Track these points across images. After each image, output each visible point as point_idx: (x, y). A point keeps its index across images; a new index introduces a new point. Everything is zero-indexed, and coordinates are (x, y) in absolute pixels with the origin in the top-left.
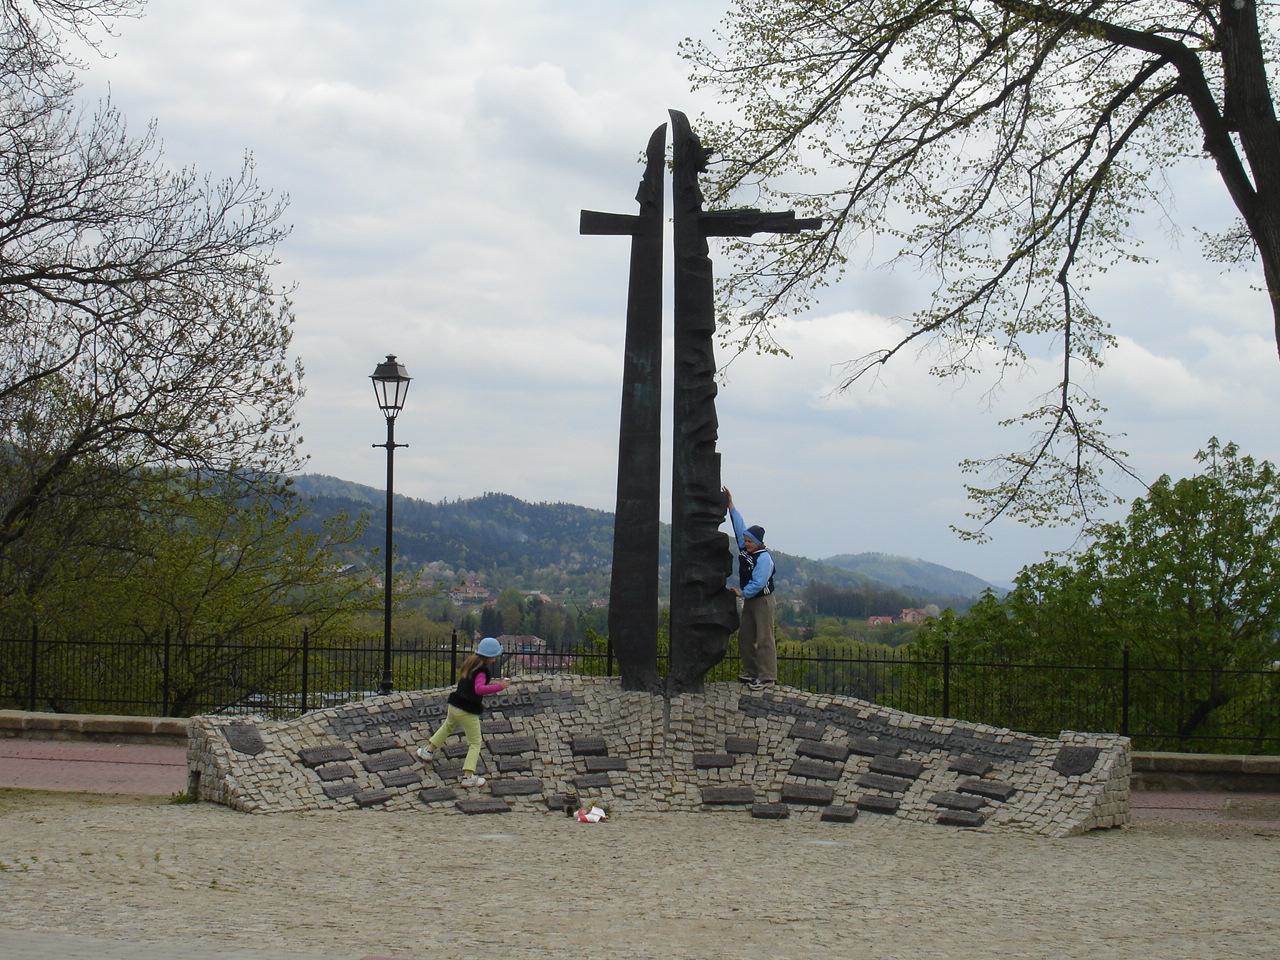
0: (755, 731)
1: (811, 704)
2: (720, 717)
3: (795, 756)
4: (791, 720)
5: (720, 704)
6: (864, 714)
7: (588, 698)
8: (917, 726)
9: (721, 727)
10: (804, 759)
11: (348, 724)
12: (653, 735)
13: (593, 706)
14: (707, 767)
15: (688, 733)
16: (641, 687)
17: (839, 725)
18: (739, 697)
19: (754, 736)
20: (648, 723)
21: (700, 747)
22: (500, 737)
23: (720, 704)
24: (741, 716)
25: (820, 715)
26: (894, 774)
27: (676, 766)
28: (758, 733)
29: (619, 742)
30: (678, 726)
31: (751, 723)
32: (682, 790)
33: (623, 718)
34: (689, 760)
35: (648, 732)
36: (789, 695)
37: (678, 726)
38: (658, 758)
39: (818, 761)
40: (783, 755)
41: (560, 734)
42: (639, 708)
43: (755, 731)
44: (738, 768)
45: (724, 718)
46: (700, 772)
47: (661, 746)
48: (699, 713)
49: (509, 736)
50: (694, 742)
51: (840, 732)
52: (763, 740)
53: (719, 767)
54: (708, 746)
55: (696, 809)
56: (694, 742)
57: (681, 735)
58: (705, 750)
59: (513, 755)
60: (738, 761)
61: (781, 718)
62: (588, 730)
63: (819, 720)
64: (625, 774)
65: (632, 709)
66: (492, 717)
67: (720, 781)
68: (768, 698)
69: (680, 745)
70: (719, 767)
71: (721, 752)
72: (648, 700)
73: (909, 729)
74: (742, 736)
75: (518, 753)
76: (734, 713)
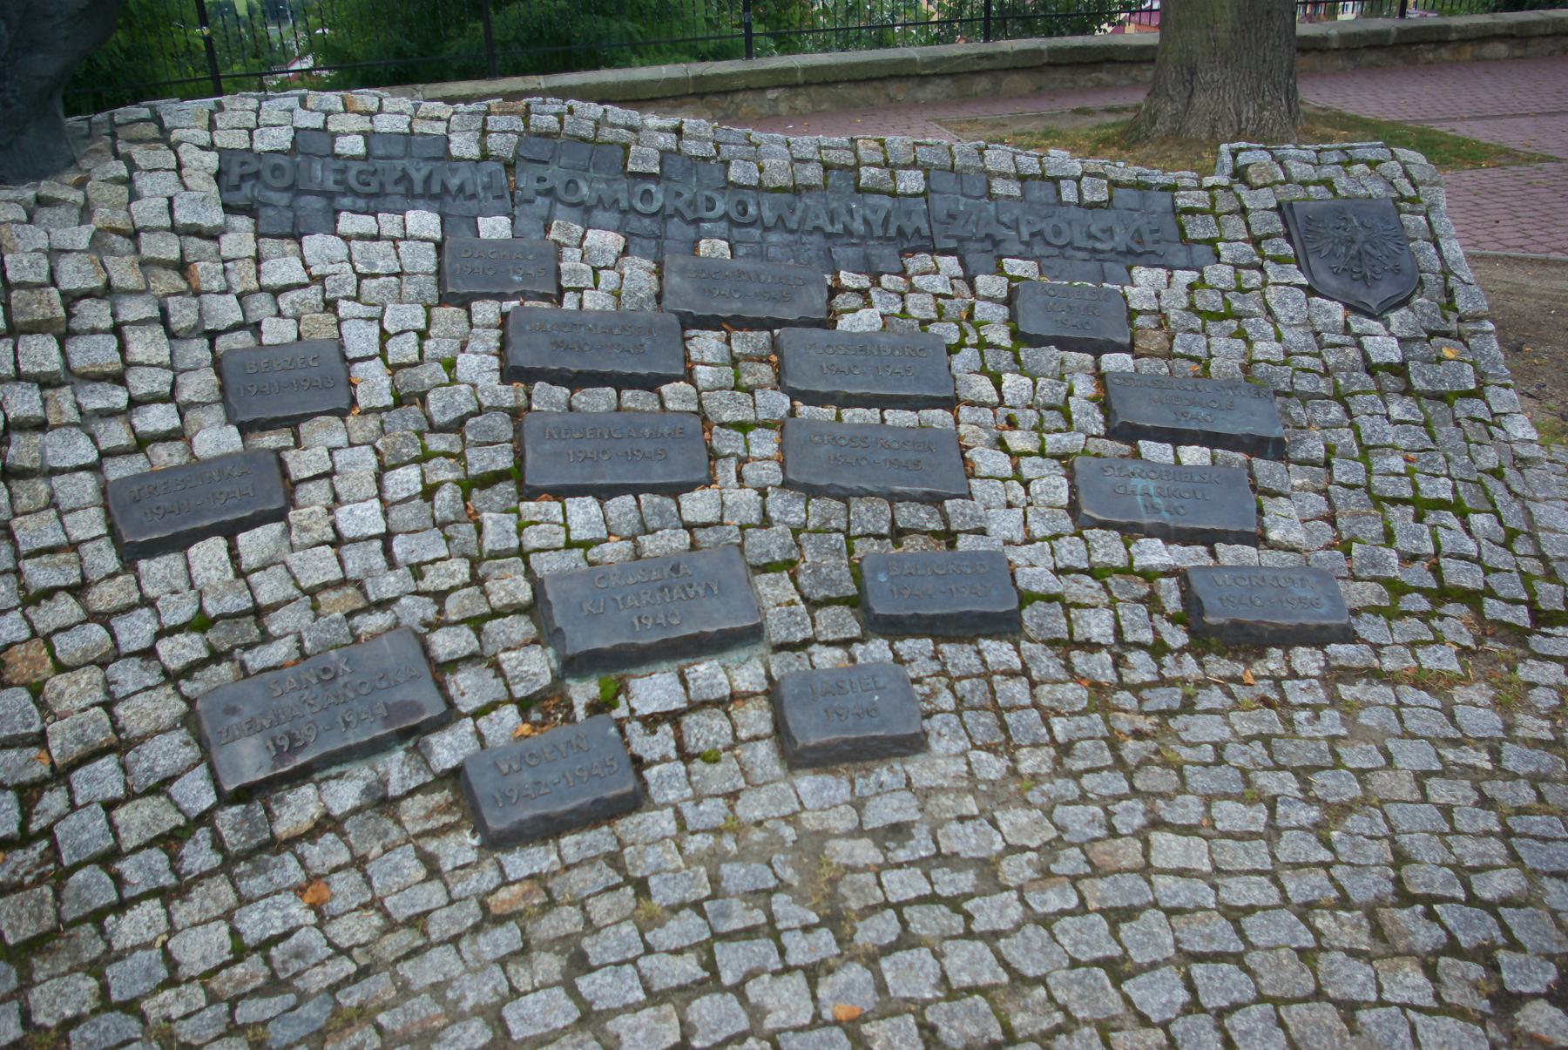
0: (313, 295)
2: (166, 265)
3: (509, 395)
4: (424, 221)
5: (149, 210)
6: (644, 159)
8: (812, 174)
10: (549, 397)
14: (180, 543)
15: (46, 383)
17: (586, 213)
18: (212, 160)
19: (320, 327)
21: (116, 434)
23: (149, 210)
24: (240, 239)
25: (505, 179)
26: (883, 402)
27: (40, 575)
28: (330, 306)
31: (283, 268)
32: (98, 729)
34: (88, 524)
36: (384, 124)
39: (599, 400)
40: (462, 400)
43: (313, 295)
45: (182, 267)
46: (156, 570)
48: (75, 275)
50: (87, 420)
52: (360, 339)
53: (229, 531)
54: (158, 418)
55: (199, 855)
56: (87, 420)
58: (142, 443)
60: (301, 464)
61: (389, 223)
63: (511, 203)
67: (258, 612)
68: (311, 144)
70: (229, 531)
71: (216, 438)
73: (796, 190)
74: (278, 331)
76: (213, 235)
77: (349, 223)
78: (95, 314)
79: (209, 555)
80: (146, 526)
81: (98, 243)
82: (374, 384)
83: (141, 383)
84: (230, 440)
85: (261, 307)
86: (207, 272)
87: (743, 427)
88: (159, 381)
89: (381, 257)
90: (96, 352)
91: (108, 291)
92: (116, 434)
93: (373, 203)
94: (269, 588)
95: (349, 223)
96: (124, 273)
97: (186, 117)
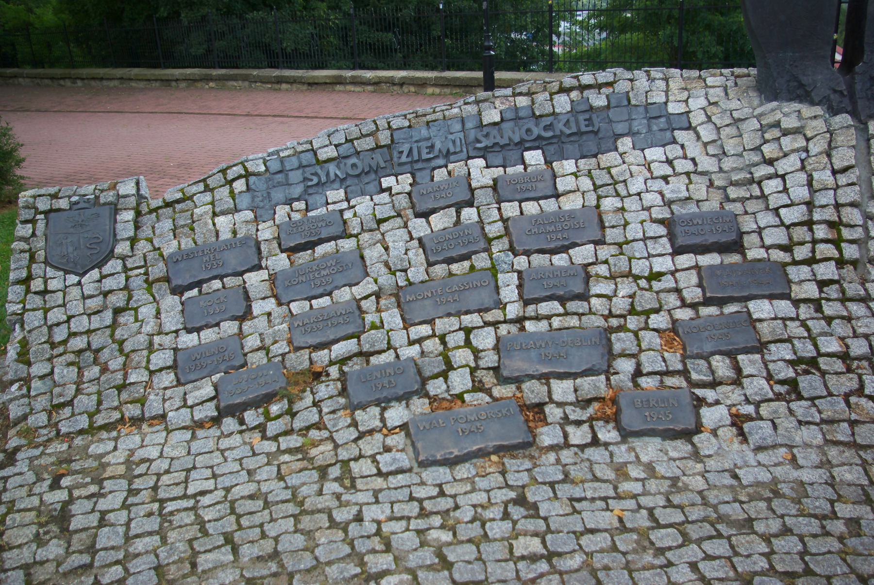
7: (697, 118)
11: (280, 184)
13: (706, 133)
16: (803, 95)
20: (824, 177)
22: (531, 208)
29: (766, 219)
33: (770, 162)
38: (854, 263)
41: (651, 198)
42: (801, 143)
47: (858, 233)
49: (550, 205)
59: (553, 252)
62: (700, 189)
65: (787, 143)
66: (523, 162)
72: (819, 125)
75: (564, 249)
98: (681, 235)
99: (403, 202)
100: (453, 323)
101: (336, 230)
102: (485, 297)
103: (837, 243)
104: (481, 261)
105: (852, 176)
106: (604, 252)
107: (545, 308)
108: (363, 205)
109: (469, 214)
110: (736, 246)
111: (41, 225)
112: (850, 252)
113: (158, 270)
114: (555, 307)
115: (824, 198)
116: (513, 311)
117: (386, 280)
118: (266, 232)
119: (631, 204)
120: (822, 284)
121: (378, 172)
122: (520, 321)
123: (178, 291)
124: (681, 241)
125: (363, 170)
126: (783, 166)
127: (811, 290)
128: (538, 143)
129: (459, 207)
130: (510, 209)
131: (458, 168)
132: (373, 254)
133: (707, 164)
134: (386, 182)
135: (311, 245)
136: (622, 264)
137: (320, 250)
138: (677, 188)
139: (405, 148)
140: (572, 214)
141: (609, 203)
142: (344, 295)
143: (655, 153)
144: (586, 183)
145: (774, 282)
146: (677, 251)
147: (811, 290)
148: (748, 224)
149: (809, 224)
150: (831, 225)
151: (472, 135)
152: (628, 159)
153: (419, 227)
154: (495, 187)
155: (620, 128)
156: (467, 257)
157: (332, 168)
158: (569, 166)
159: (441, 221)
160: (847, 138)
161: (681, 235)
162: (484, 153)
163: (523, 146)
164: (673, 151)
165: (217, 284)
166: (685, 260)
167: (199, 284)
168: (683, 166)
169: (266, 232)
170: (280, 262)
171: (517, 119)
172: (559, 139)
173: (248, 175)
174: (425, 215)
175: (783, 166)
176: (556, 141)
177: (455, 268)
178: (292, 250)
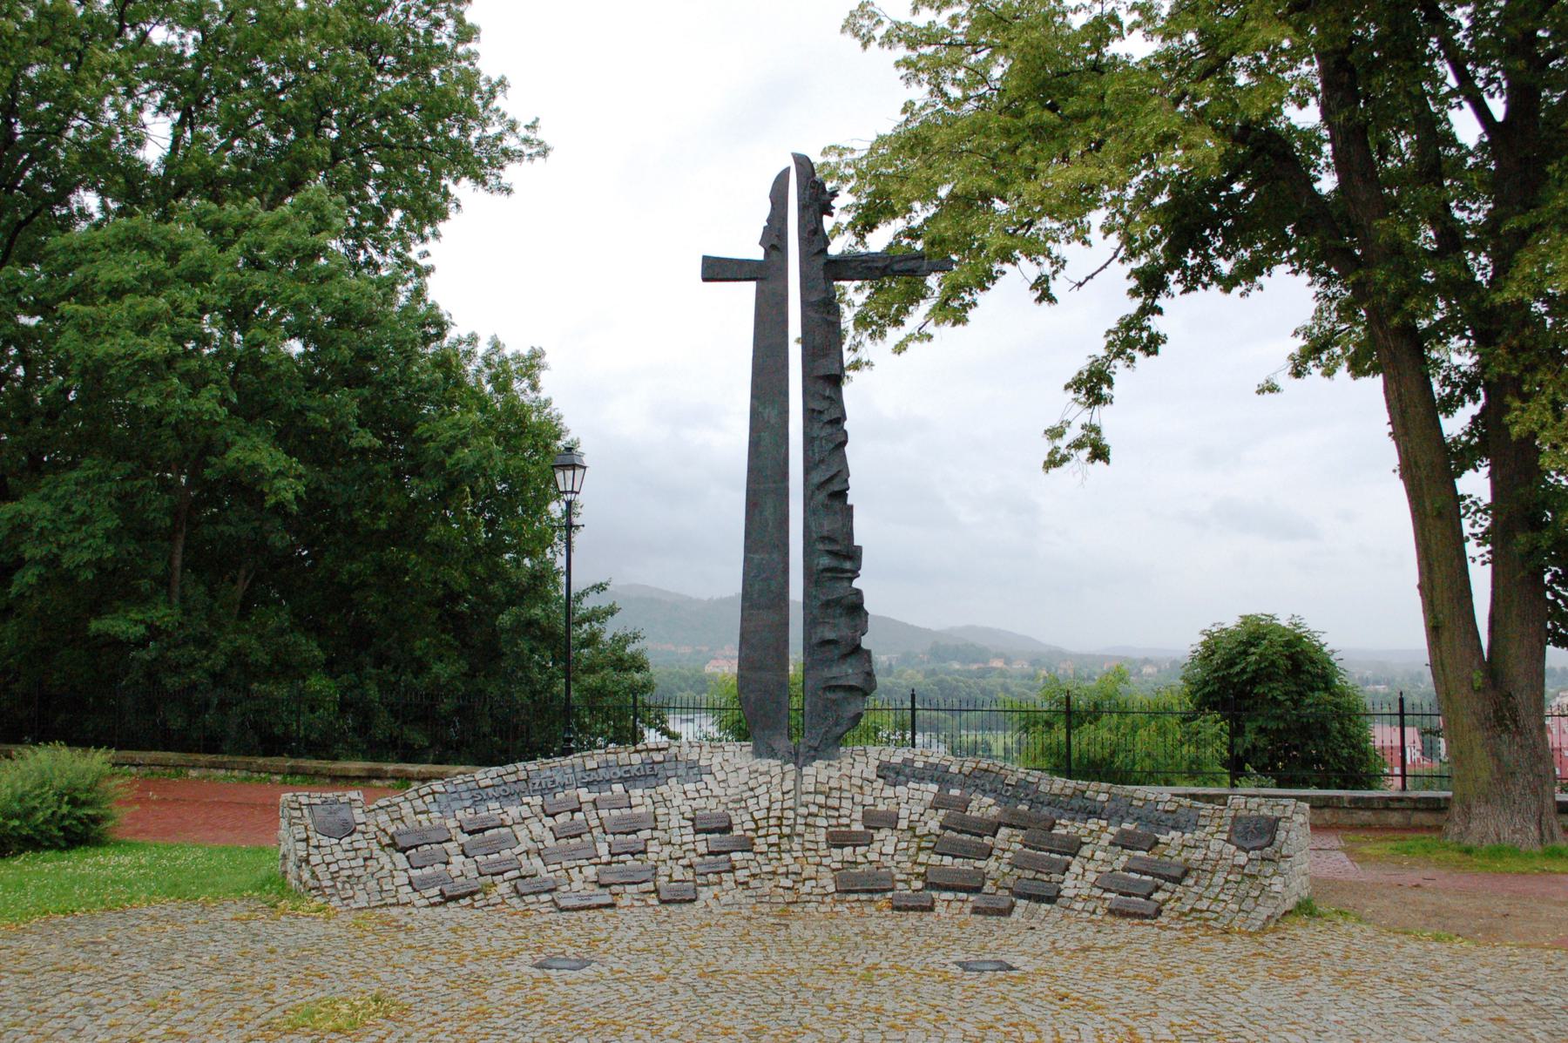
1: (954, 769)
4: (934, 788)
9: (858, 799)
12: (783, 809)
14: (842, 847)
15: (820, 806)
16: (773, 754)
17: (984, 793)
20: (778, 795)
21: (834, 822)
22: (615, 812)
30: (810, 798)
31: (889, 792)
34: (822, 838)
35: (777, 806)
37: (810, 798)
38: (788, 836)
41: (683, 809)
44: (876, 846)
48: (833, 783)
49: (626, 811)
51: (989, 800)
52: (903, 813)
53: (855, 846)
54: (845, 821)
56: (827, 817)
57: (814, 809)
58: (839, 825)
60: (876, 837)
61: (922, 786)
63: (963, 786)
64: (749, 855)
65: (761, 779)
69: (810, 820)
71: (858, 827)
72: (778, 770)
74: (881, 807)
75: (635, 832)
77: (911, 785)
78: (836, 794)
79: (848, 850)
80: (838, 840)
81: (840, 777)
82: (903, 824)
83: (842, 812)
84: (862, 828)
85: (879, 801)
86: (867, 789)
87: (1004, 850)
88: (847, 813)
89: (918, 795)
90: (836, 803)
91: (840, 789)
92: (834, 822)
93: (921, 780)
94: (860, 859)
95: (911, 785)
96: (845, 785)
97: (873, 751)
98: (701, 826)
99: (539, 809)
100: (573, 864)
101: (498, 822)
102: (590, 853)
103: (779, 826)
104: (587, 837)
105: (791, 794)
106: (656, 834)
107: (622, 858)
108: (514, 811)
109: (579, 816)
110: (728, 829)
111: (306, 812)
112: (786, 830)
113: (386, 840)
114: (629, 857)
115: (775, 806)
116: (605, 859)
117: (530, 844)
118: (451, 823)
119: (674, 812)
120: (770, 845)
121: (520, 794)
122: (609, 863)
123: (404, 850)
124: (699, 827)
125: (508, 795)
126: (757, 792)
127: (765, 848)
128: (623, 780)
129: (573, 812)
130: (603, 813)
131: (570, 792)
132: (522, 833)
133: (718, 791)
134: (525, 800)
135: (482, 830)
136: (667, 837)
137: (487, 833)
138: (700, 803)
139: (537, 781)
140: (639, 816)
141: (660, 811)
142: (506, 853)
143: (689, 787)
144: (649, 801)
145: (747, 845)
146: (697, 832)
147: (765, 848)
148: (736, 820)
149: (768, 818)
150: (779, 818)
151: (579, 775)
152: (672, 789)
153: (549, 822)
154: (594, 802)
155: (669, 773)
156: (579, 836)
157: (490, 790)
158: (639, 792)
159: (560, 819)
160: (791, 776)
161: (701, 826)
162: (587, 784)
163: (610, 781)
164: (701, 785)
165: (427, 847)
166: (700, 837)
167: (416, 847)
168: (703, 793)
169: (451, 823)
170: (465, 838)
171: (608, 767)
172: (634, 778)
173: (434, 793)
174: (553, 816)
175: (757, 792)
176: (629, 780)
177: (572, 841)
178: (471, 833)
